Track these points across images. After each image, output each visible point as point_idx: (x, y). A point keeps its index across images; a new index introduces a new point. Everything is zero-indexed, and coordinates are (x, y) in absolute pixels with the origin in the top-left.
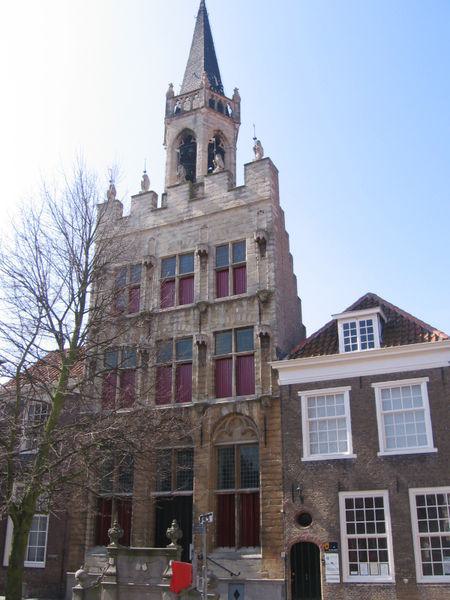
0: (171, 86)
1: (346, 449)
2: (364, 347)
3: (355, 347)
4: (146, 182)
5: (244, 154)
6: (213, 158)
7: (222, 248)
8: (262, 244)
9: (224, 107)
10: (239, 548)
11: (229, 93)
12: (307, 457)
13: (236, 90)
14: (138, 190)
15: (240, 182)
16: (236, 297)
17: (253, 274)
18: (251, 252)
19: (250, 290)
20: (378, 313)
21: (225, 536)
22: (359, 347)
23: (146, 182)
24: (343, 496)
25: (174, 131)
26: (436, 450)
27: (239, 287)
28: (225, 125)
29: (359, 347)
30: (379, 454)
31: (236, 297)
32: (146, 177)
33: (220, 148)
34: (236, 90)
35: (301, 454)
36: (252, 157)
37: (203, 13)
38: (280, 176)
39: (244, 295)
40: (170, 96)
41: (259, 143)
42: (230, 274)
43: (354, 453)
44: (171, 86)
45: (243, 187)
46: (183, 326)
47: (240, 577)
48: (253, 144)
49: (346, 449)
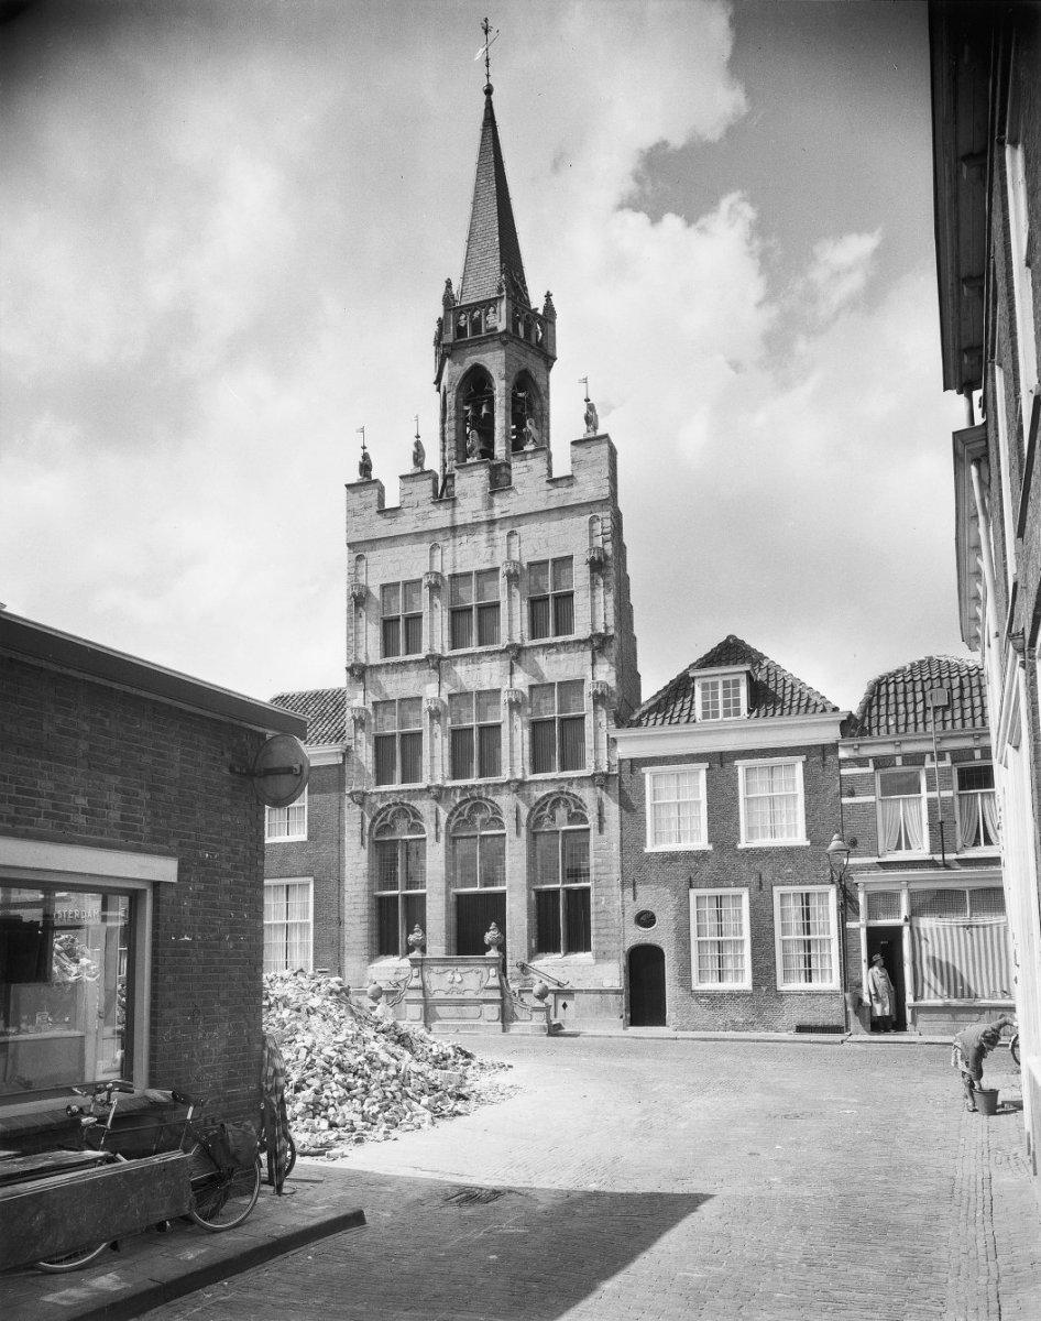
0: (449, 284)
1: (700, 842)
2: (727, 714)
3: (716, 715)
4: (418, 457)
5: (564, 421)
6: (525, 426)
7: (538, 566)
8: (597, 566)
9: (532, 335)
10: (565, 954)
11: (537, 303)
12: (648, 849)
13: (548, 296)
14: (409, 467)
15: (561, 467)
16: (560, 639)
17: (581, 603)
18: (580, 575)
19: (581, 630)
20: (748, 672)
21: (545, 941)
22: (721, 714)
23: (418, 457)
24: (693, 893)
25: (454, 371)
26: (808, 843)
27: (564, 625)
28: (533, 363)
29: (721, 714)
30: (740, 846)
31: (560, 639)
32: (418, 444)
33: (529, 402)
34: (548, 296)
35: (643, 841)
36: (581, 431)
37: (490, 121)
38: (619, 456)
39: (570, 638)
40: (448, 300)
41: (591, 408)
42: (550, 611)
43: (709, 842)
44: (449, 284)
45: (572, 476)
46: (487, 674)
47: (566, 987)
48: (584, 409)
49: (700, 842)
